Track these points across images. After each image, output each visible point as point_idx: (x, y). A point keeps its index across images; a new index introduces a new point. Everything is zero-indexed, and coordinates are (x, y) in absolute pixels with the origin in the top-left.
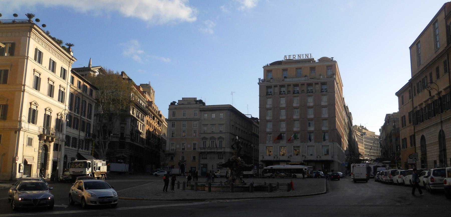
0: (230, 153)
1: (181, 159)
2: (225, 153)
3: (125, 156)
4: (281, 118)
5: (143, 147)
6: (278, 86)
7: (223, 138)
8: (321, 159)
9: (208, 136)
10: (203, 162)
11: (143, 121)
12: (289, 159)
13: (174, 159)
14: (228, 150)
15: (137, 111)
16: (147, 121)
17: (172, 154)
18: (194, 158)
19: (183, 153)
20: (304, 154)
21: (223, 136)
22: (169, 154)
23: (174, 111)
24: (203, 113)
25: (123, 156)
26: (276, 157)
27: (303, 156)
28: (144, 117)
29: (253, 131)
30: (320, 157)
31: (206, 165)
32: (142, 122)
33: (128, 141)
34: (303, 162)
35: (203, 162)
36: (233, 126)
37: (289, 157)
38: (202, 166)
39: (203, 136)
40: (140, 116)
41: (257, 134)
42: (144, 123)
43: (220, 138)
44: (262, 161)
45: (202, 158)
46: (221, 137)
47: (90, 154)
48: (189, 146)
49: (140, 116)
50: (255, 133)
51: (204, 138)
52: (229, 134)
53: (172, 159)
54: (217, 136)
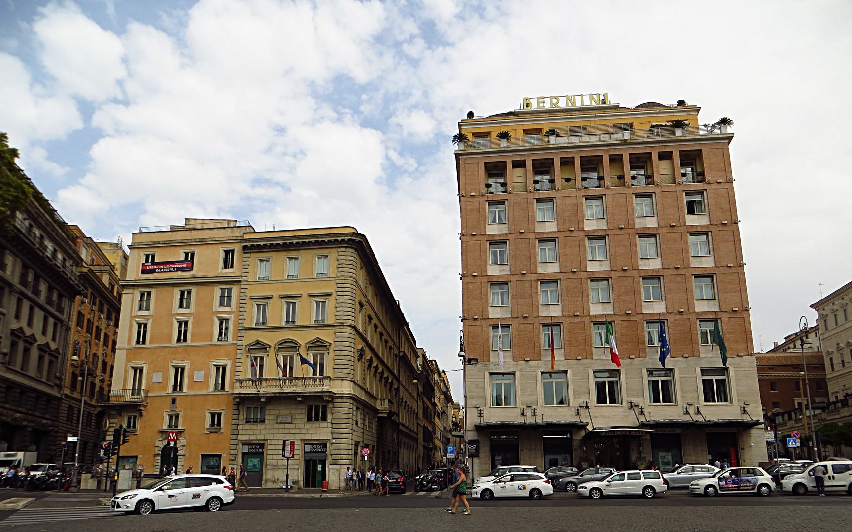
0: (353, 398)
1: (165, 427)
2: (333, 396)
4: (540, 270)
5: (55, 392)
6: (529, 164)
7: (325, 346)
8: (700, 418)
9: (270, 339)
10: (250, 433)
14: (346, 388)
15: (25, 267)
16: (80, 314)
18: (216, 419)
19: (174, 401)
20: (635, 400)
21: (326, 335)
24: (254, 257)
26: (529, 413)
27: (632, 406)
28: (65, 303)
30: (698, 412)
35: (250, 433)
37: (578, 414)
38: (246, 449)
42: (64, 317)
43: (318, 345)
44: (479, 428)
45: (248, 422)
46: (318, 340)
48: (199, 376)
51: (259, 347)
52: (349, 330)
54: (303, 338)
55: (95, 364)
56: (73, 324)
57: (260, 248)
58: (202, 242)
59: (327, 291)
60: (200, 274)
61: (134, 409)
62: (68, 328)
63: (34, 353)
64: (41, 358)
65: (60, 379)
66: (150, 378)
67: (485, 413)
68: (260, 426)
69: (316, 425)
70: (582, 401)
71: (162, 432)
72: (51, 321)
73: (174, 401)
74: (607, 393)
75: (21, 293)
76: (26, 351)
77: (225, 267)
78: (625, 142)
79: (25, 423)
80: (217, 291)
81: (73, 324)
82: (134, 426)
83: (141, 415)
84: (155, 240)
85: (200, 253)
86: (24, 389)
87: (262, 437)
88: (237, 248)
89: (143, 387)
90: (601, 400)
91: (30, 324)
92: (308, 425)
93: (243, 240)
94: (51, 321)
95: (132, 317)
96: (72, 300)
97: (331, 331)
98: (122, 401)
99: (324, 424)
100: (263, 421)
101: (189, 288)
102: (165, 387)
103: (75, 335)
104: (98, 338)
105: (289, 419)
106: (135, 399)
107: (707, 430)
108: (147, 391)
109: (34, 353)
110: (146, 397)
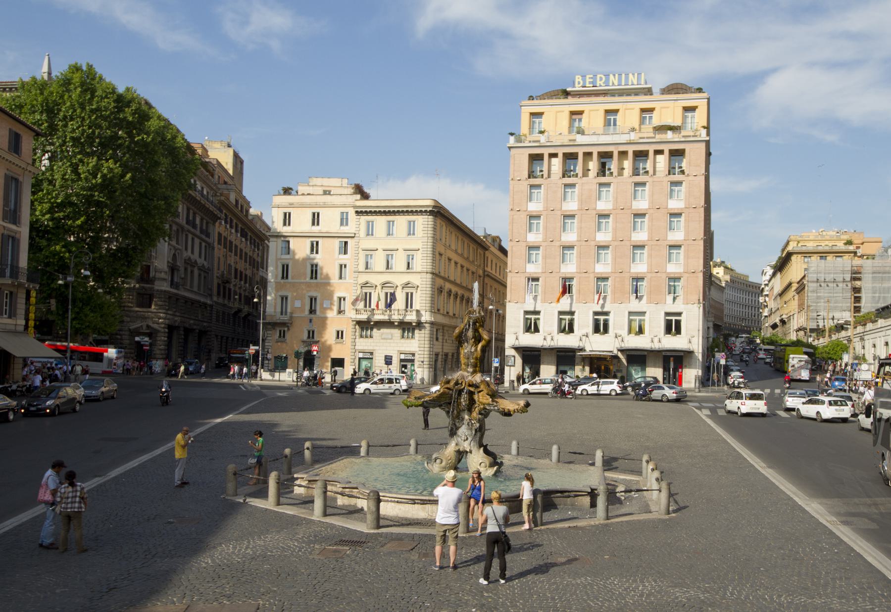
3: (155, 326)
5: (209, 302)
10: (364, 344)
11: (208, 235)
12: (581, 345)
13: (288, 336)
15: (188, 209)
16: (220, 234)
17: (284, 324)
19: (311, 321)
20: (619, 332)
22: (274, 325)
23: (287, 210)
24: (364, 219)
25: (148, 327)
26: (549, 338)
28: (211, 226)
29: (489, 269)
31: (372, 353)
32: (204, 237)
33: (165, 286)
34: (615, 352)
36: (441, 255)
38: (361, 355)
39: (363, 279)
40: (198, 221)
41: (501, 277)
42: (210, 240)
47: (22, 328)
49: (198, 221)
50: (494, 273)
53: (282, 335)
55: (229, 272)
56: (216, 244)
57: (367, 213)
58: (325, 206)
59: (416, 247)
60: (324, 230)
61: (282, 327)
62: (213, 248)
63: (196, 272)
64: (200, 275)
65: (211, 290)
66: (293, 303)
67: (520, 338)
68: (370, 340)
69: (408, 341)
70: (584, 332)
71: (304, 342)
72: (197, 241)
73: (311, 321)
74: (600, 327)
75: (189, 231)
76: (192, 272)
77: (342, 224)
78: (630, 143)
79: (195, 327)
80: (337, 242)
81: (216, 244)
82: (284, 336)
83: (289, 329)
84: (291, 201)
85: (324, 214)
86: (187, 300)
87: (371, 348)
88: (351, 212)
89: (289, 310)
90: (597, 330)
91: (192, 252)
92: (403, 341)
93: (354, 207)
94: (203, 244)
95: (277, 260)
96: (215, 222)
97: (419, 276)
98: (274, 320)
99: (413, 341)
100: (371, 337)
101: (317, 239)
102: (303, 311)
103: (219, 251)
104: (231, 251)
105: (390, 337)
106: (285, 318)
107: (664, 354)
108: (291, 313)
109: (196, 272)
110: (291, 317)
